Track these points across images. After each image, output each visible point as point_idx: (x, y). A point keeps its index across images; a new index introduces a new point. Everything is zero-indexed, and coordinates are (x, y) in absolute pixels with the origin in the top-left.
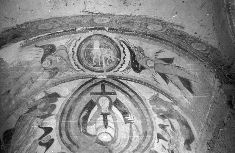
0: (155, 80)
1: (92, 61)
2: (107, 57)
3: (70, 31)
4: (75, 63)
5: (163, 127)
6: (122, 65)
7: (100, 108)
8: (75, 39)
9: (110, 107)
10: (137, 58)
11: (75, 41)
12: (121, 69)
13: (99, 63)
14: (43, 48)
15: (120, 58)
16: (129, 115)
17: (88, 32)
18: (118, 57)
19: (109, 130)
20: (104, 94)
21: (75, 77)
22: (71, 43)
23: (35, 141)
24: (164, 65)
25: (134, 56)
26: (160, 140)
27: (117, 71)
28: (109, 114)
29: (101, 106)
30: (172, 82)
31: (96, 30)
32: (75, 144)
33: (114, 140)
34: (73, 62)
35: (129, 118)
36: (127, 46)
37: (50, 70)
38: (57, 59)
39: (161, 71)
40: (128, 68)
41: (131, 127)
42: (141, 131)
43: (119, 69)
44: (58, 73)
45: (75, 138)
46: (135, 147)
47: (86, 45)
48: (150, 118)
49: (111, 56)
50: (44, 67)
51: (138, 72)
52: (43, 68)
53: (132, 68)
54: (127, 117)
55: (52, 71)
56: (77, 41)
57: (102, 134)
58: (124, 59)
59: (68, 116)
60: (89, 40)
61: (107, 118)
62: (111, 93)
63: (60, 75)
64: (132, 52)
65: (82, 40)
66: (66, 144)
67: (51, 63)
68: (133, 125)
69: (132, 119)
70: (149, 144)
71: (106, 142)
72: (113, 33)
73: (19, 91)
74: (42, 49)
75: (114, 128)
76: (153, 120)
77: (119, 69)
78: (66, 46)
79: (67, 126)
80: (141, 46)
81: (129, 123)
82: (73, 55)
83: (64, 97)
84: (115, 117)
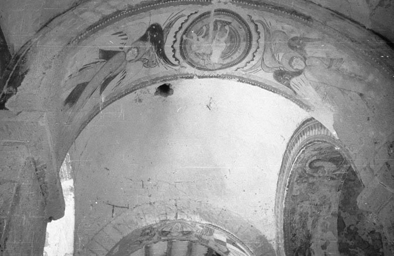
4: (259, 37)
6: (180, 28)
8: (243, 71)
11: (245, 68)
12: (182, 20)
13: (219, 27)
22: (251, 69)
24: (111, 73)
25: (158, 52)
27: (191, 14)
30: (93, 63)
37: (299, 51)
40: (170, 25)
43: (186, 21)
44: (293, 35)
47: (232, 58)
52: (306, 62)
53: (163, 28)
55: (298, 47)
56: (243, 68)
58: (175, 39)
64: (163, 56)
65: (235, 67)
67: (292, 59)
72: (188, 74)
73: (353, 75)
74: (291, 85)
77: (186, 21)
78: (260, 68)
82: (256, 51)
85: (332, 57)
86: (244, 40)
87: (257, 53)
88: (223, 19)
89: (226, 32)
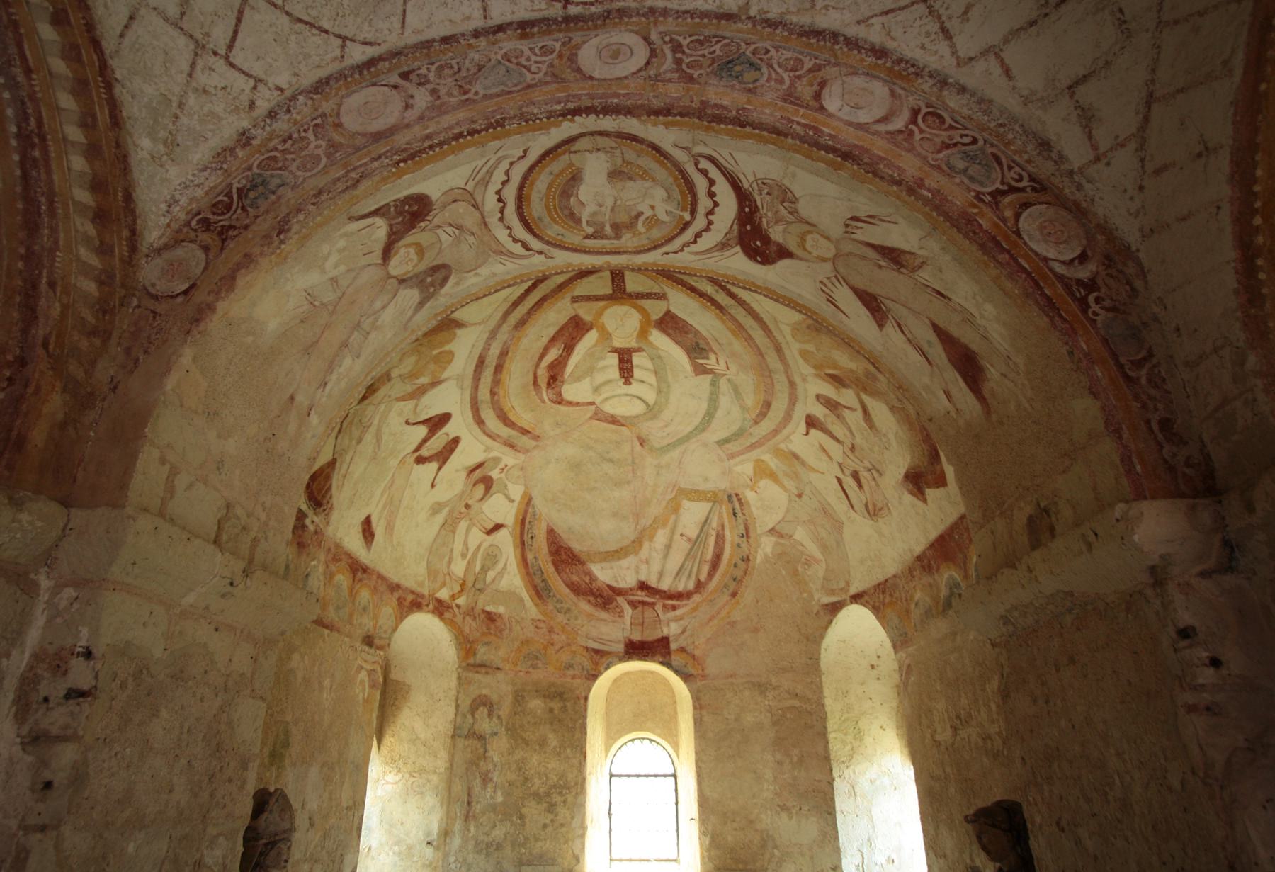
0: (828, 300)
1: (578, 221)
2: (641, 208)
3: (483, 133)
5: (832, 405)
6: (698, 235)
7: (605, 335)
8: (504, 157)
9: (643, 334)
10: (764, 220)
11: (505, 165)
12: (693, 248)
13: (608, 229)
14: (383, 215)
15: (693, 213)
16: (712, 357)
17: (559, 125)
18: (684, 209)
19: (635, 388)
20: (622, 298)
21: (516, 277)
22: (490, 173)
23: (402, 461)
25: (755, 210)
26: (813, 432)
27: (676, 253)
28: (639, 350)
29: (610, 330)
31: (593, 117)
32: (525, 432)
33: (652, 411)
34: (502, 235)
35: (710, 362)
36: (728, 179)
38: (444, 237)
39: (861, 284)
40: (723, 246)
41: (714, 384)
42: (750, 401)
43: (686, 245)
44: (452, 281)
45: (524, 417)
46: (723, 434)
48: (786, 372)
49: (652, 203)
50: (395, 277)
51: (762, 263)
54: (703, 358)
55: (429, 279)
56: (512, 164)
57: (616, 399)
58: (710, 217)
59: (499, 368)
60: (564, 153)
61: (630, 361)
62: (648, 296)
63: (457, 284)
64: (743, 196)
65: (533, 156)
66: (499, 436)
67: (421, 251)
68: (723, 383)
69: (722, 365)
70: (775, 432)
71: (627, 417)
72: (667, 125)
75: (655, 383)
76: (797, 379)
77: (686, 245)
78: (470, 187)
79: (496, 397)
80: (786, 182)
81: (711, 376)
82: (502, 211)
83: (480, 324)
84: (660, 357)
85: (373, 336)
86: (540, 219)
87: (498, 209)
88: (605, 242)
89: (588, 222)
